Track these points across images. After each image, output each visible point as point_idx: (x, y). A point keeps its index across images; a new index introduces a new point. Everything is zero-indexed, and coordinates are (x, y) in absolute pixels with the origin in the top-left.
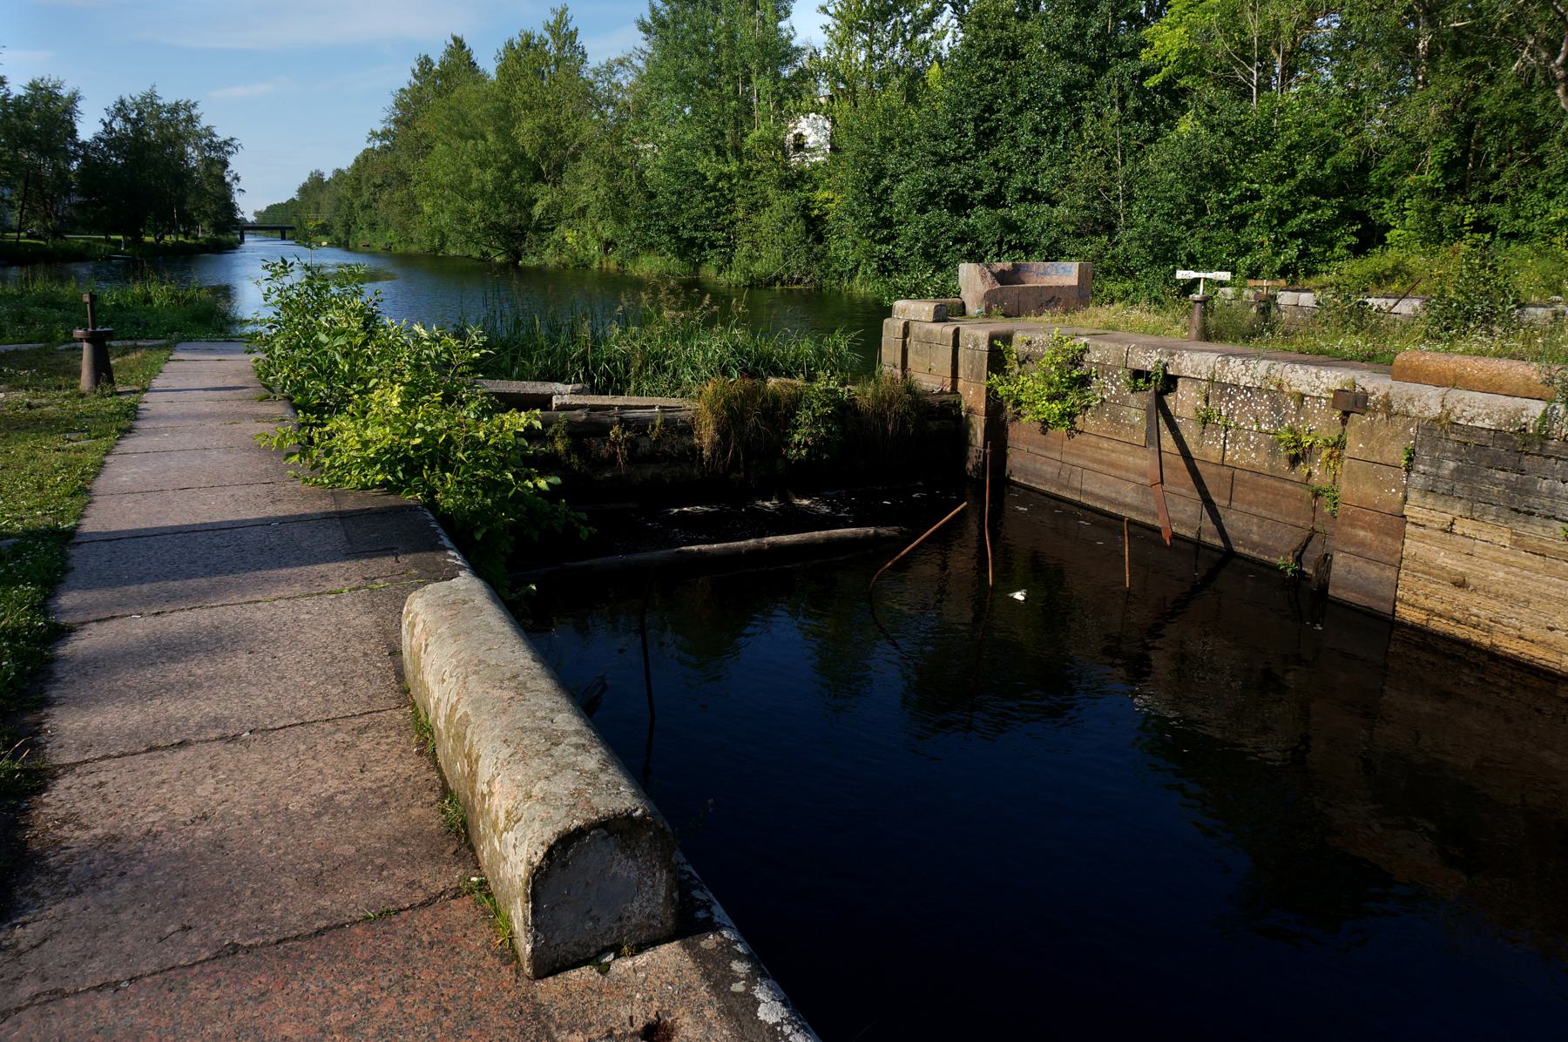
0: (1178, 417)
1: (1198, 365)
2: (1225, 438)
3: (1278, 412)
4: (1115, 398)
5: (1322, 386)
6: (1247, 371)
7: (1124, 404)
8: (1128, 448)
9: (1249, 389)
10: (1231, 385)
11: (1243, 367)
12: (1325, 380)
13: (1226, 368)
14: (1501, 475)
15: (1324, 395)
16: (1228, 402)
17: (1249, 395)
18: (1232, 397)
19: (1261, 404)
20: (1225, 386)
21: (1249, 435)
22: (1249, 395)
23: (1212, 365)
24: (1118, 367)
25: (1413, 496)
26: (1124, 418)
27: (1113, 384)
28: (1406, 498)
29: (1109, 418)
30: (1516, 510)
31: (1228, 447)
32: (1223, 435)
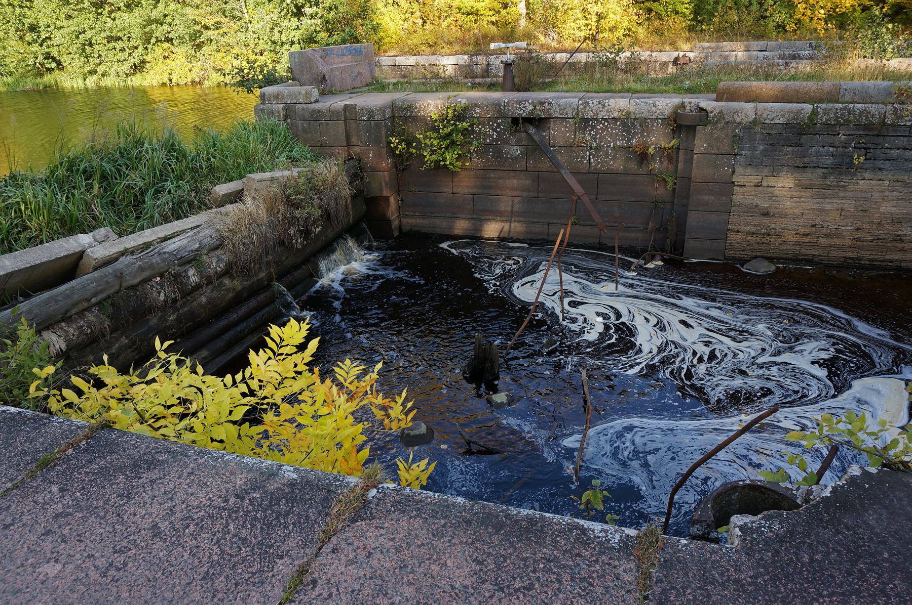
0: (552, 146)
1: (565, 108)
2: (590, 155)
3: (629, 132)
4: (496, 140)
5: (658, 112)
6: (603, 108)
7: (507, 143)
8: (512, 173)
9: (606, 120)
10: (592, 119)
11: (600, 105)
12: (660, 107)
13: (588, 108)
14: (790, 149)
15: (660, 117)
16: (590, 131)
17: (606, 124)
18: (593, 127)
19: (616, 129)
20: (587, 121)
21: (607, 150)
22: (606, 124)
23: (576, 107)
24: (498, 118)
25: (739, 169)
26: (506, 153)
27: (494, 130)
28: (733, 172)
29: (493, 156)
30: (797, 167)
31: (592, 160)
32: (588, 154)
